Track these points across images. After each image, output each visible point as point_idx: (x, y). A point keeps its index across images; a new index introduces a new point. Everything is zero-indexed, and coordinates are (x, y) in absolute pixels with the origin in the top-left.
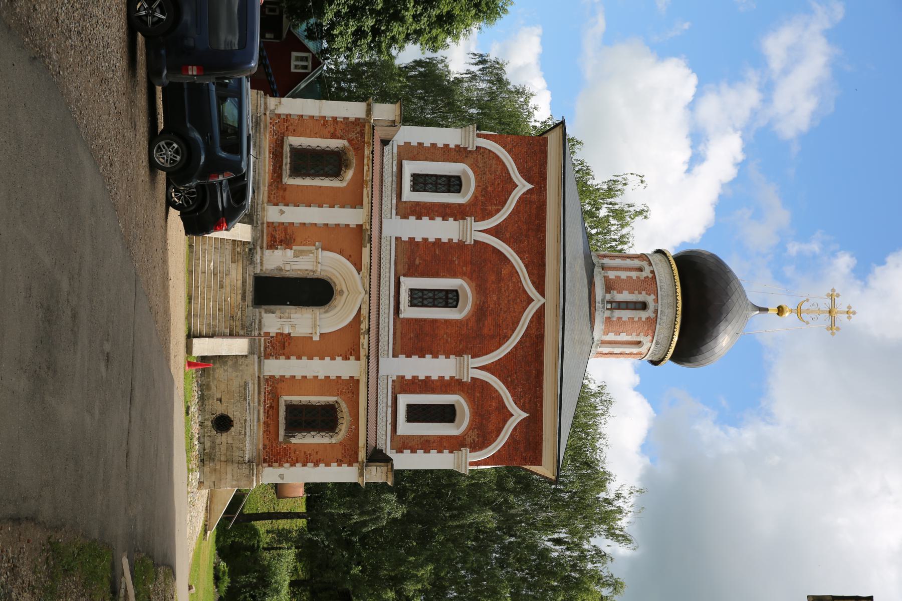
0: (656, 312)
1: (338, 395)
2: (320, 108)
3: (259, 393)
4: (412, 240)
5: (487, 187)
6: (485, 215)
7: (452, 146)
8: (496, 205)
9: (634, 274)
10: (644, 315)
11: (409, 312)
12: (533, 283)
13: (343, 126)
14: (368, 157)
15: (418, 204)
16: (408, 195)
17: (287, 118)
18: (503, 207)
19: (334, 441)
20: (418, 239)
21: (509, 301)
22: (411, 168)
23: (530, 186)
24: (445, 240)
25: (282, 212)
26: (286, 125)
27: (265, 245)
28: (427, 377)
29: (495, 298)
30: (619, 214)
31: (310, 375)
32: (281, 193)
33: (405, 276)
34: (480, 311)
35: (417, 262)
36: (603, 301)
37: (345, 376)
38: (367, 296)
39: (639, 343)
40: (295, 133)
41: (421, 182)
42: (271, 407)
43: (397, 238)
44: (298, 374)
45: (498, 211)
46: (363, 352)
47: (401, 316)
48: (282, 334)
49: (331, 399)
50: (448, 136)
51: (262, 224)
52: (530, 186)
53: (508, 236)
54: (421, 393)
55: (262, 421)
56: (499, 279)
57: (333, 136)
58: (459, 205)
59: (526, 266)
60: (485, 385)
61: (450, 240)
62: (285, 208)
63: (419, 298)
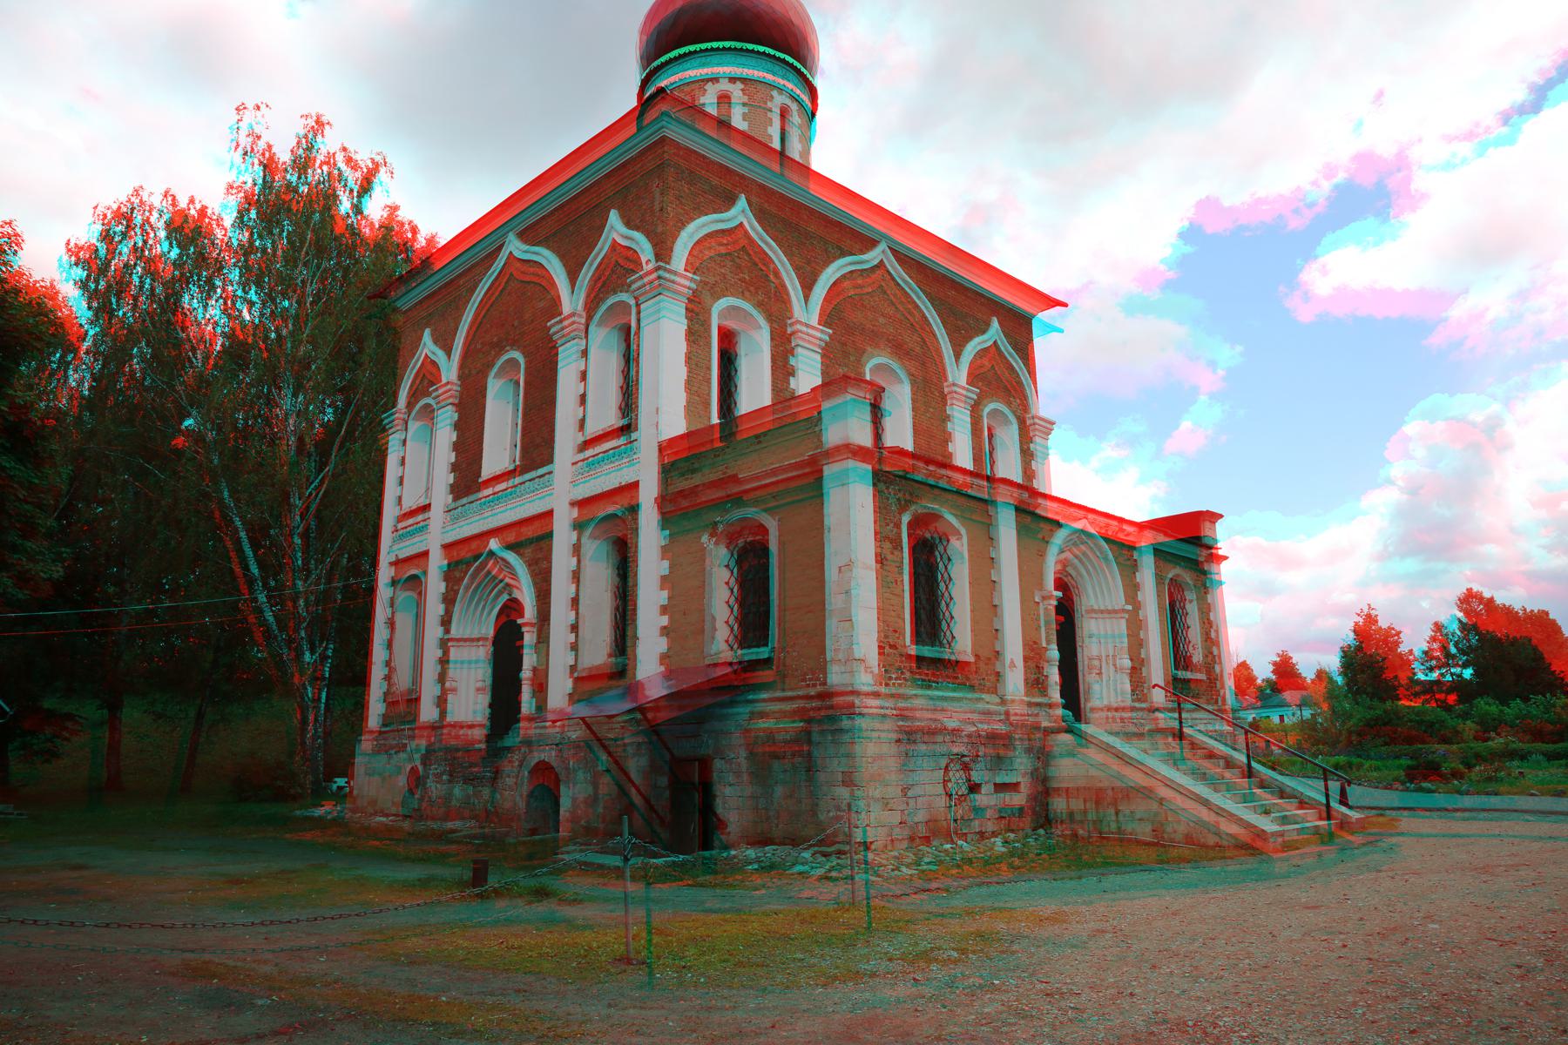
6: (781, 296)
12: (862, 252)
14: (931, 474)
26: (887, 650)
29: (882, 320)
32: (982, 665)
34: (899, 350)
38: (1090, 516)
45: (777, 273)
51: (1030, 704)
59: (844, 254)
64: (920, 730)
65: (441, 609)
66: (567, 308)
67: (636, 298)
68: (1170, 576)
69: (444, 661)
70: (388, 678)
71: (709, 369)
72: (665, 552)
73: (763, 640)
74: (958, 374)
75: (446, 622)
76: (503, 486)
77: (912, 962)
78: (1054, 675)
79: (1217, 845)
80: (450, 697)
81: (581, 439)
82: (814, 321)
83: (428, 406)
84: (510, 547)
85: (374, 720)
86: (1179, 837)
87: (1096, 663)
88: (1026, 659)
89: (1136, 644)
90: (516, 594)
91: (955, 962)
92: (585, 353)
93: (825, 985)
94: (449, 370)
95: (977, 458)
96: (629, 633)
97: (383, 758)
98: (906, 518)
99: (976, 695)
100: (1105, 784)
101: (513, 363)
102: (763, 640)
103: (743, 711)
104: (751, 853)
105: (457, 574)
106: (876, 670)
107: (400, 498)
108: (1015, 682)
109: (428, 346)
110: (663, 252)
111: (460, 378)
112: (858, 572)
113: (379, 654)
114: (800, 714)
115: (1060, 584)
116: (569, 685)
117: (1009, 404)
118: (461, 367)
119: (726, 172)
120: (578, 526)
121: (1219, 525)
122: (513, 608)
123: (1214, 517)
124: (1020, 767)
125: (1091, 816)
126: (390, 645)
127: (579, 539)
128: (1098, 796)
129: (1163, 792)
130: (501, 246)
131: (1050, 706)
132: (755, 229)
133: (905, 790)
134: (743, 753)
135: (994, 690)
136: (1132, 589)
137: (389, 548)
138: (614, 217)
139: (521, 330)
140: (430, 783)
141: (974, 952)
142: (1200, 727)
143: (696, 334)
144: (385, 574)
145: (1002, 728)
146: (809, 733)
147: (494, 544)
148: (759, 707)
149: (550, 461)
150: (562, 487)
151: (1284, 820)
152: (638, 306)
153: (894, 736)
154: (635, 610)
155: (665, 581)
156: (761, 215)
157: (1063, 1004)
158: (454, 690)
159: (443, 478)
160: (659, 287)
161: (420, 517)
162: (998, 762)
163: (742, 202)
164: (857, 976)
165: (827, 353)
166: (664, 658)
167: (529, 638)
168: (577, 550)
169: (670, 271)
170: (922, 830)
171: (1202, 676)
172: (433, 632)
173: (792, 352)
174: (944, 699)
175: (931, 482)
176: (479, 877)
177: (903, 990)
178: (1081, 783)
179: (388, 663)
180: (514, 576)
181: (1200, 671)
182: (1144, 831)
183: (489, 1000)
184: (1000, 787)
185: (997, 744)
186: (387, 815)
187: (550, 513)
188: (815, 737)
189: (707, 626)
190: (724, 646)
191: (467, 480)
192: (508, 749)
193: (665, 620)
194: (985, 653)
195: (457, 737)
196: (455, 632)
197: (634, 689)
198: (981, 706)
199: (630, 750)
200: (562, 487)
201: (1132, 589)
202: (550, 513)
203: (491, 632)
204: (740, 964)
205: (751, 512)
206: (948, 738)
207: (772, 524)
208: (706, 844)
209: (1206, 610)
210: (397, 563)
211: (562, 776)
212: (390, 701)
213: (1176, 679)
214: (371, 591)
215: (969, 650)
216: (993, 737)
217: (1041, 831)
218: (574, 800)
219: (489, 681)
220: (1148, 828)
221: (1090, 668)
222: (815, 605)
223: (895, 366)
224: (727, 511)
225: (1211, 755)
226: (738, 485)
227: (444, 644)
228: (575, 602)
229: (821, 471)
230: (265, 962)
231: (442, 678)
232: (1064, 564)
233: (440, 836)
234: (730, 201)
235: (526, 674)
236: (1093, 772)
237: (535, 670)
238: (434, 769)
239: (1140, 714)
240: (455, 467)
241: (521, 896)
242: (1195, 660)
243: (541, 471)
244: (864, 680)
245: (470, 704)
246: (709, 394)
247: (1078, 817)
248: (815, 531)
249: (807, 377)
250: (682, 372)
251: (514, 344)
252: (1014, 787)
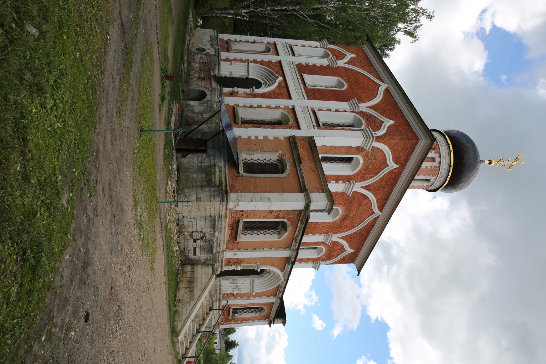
5: (369, 166)
6: (363, 179)
12: (378, 206)
14: (300, 228)
18: (375, 176)
25: (236, 254)
26: (241, 213)
27: (223, 265)
29: (354, 213)
30: (416, 11)
32: (236, 244)
34: (344, 218)
38: (285, 282)
51: (222, 261)
59: (377, 200)
64: (215, 223)
65: (259, 60)
66: (361, 105)
67: (363, 130)
69: (241, 61)
70: (236, 41)
71: (339, 154)
72: (276, 138)
73: (246, 171)
74: (335, 238)
75: (254, 61)
76: (300, 82)
77: (140, 223)
78: (232, 268)
79: (174, 321)
80: (229, 63)
81: (315, 109)
82: (354, 190)
83: (329, 55)
84: (280, 84)
85: (221, 36)
86: (177, 308)
87: (236, 282)
88: (237, 259)
89: (242, 296)
90: (263, 86)
91: (140, 237)
92: (345, 111)
93: (133, 196)
94: (341, 63)
95: (306, 244)
96: (249, 125)
97: (209, 39)
98: (285, 220)
100: (195, 284)
101: (343, 86)
102: (246, 171)
103: (222, 164)
104: (175, 166)
105: (271, 65)
106: (235, 209)
107: (297, 46)
108: (229, 255)
109: (350, 56)
110: (379, 139)
111: (338, 67)
112: (268, 204)
113: (244, 38)
114: (221, 184)
115: (262, 271)
116: (232, 104)
117: (324, 255)
118: (342, 67)
119: (406, 160)
120: (286, 108)
121: (281, 325)
122: (258, 85)
123: (284, 323)
124: (202, 256)
125: (185, 279)
126: (248, 42)
127: (281, 108)
128: (191, 282)
129: (192, 303)
130: (383, 82)
131: (221, 267)
132: (386, 171)
133: (194, 218)
134: (208, 164)
135: (227, 248)
136: (260, 295)
137: (280, 42)
138: (392, 122)
139: (355, 89)
140: (200, 55)
141: (142, 243)
142: (214, 316)
143: (350, 149)
144: (271, 40)
145: (214, 251)
146: (214, 186)
147: (280, 79)
148: (223, 170)
149: (309, 99)
150: (300, 102)
151: (182, 343)
152: (360, 130)
153: (212, 215)
154: (256, 127)
155: (266, 138)
156: (391, 172)
157: (127, 272)
158: (231, 64)
159: (304, 61)
160: (367, 137)
161: (290, 53)
162: (203, 249)
163: (396, 166)
164: (136, 205)
165: (342, 194)
166: (240, 137)
167: (248, 91)
168: (278, 107)
169: (372, 141)
170: (181, 224)
171: (230, 317)
172: (251, 57)
173: (343, 182)
174: (225, 231)
175: (298, 229)
176: (168, 77)
177: (132, 221)
178: (196, 276)
179: (241, 41)
180: (269, 85)
181: (232, 316)
182: (179, 297)
183: (130, 88)
184: (195, 249)
185: (210, 249)
186: (189, 40)
187: (290, 98)
188: (213, 189)
189: (250, 153)
190: (244, 158)
191: (303, 69)
192: (211, 83)
193: (253, 138)
194: (239, 245)
195: (215, 65)
196: (251, 65)
197: (229, 127)
198: (222, 244)
199: (209, 125)
200: (300, 102)
201: (260, 295)
202: (290, 98)
203: (251, 77)
204: (140, 168)
205: (289, 168)
207: (284, 175)
208: (178, 151)
209: (253, 319)
210: (275, 44)
211: (201, 101)
212: (227, 42)
213: (230, 308)
214: (266, 35)
215: (241, 240)
216: (212, 248)
217: (180, 262)
218: (193, 106)
219: (234, 76)
220: (181, 298)
221: (234, 280)
222: (257, 189)
223: (338, 217)
224: (289, 160)
225: (204, 319)
226: (299, 163)
227: (247, 61)
228: (260, 107)
229: (302, 192)
230: (143, 13)
231: (235, 60)
232: (269, 272)
233: (182, 59)
234: (396, 162)
235: (236, 89)
236: (199, 280)
237: (237, 92)
238: (205, 57)
239: (218, 296)
240: (307, 65)
241: (162, 92)
242: (236, 315)
243: (305, 95)
244: (231, 205)
245: (226, 70)
246: (330, 154)
247: (185, 275)
248: (283, 190)
249: (334, 187)
250: (337, 145)
251: (350, 86)
252: (195, 254)
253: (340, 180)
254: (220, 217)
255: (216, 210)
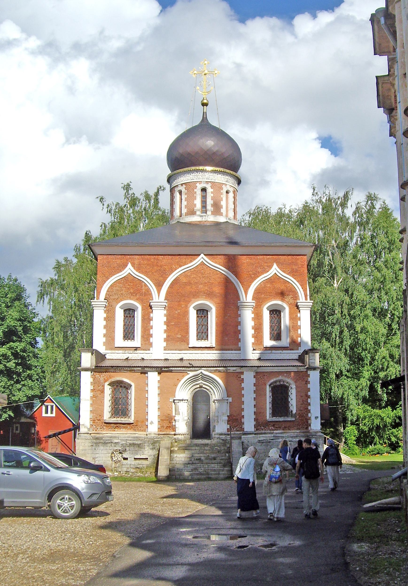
0: (207, 182)
1: (265, 385)
2: (86, 400)
3: (265, 433)
4: (166, 340)
6: (148, 293)
7: (105, 315)
8: (142, 286)
9: (184, 197)
10: (210, 190)
11: (212, 341)
13: (96, 385)
15: (142, 337)
16: (137, 342)
17: (93, 421)
19: (294, 386)
20: (165, 336)
21: (203, 277)
22: (119, 341)
23: (130, 265)
24: (165, 319)
25: (152, 423)
28: (253, 328)
31: (253, 403)
33: (188, 344)
35: (180, 336)
36: (201, 216)
37: (254, 381)
39: (227, 192)
40: (102, 415)
41: (129, 334)
42: (273, 426)
43: (165, 350)
44: (253, 410)
45: (146, 285)
46: (238, 370)
47: (214, 346)
48: (228, 421)
49: (268, 389)
50: (99, 316)
51: (159, 434)
52: (130, 265)
53: (161, 278)
54: (262, 332)
55: (283, 431)
56: (189, 283)
57: (103, 391)
58: (143, 310)
59: (181, 266)
60: (258, 292)
61: (165, 315)
62: (149, 421)
63: (202, 334)
64: (102, 443)
68: (272, 381)
99: (135, 432)
153: (90, 444)
185: (137, 446)
206: (113, 445)
253: (149, 316)
254: (97, 439)
255: (84, 442)
